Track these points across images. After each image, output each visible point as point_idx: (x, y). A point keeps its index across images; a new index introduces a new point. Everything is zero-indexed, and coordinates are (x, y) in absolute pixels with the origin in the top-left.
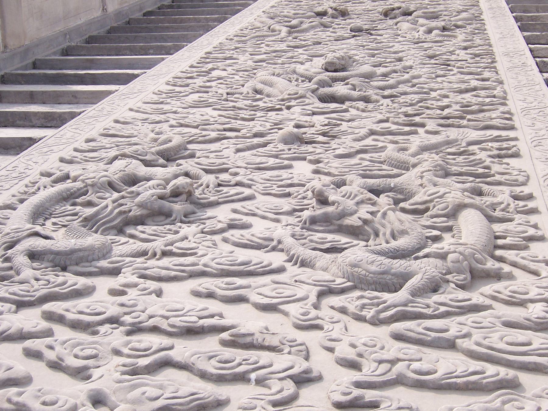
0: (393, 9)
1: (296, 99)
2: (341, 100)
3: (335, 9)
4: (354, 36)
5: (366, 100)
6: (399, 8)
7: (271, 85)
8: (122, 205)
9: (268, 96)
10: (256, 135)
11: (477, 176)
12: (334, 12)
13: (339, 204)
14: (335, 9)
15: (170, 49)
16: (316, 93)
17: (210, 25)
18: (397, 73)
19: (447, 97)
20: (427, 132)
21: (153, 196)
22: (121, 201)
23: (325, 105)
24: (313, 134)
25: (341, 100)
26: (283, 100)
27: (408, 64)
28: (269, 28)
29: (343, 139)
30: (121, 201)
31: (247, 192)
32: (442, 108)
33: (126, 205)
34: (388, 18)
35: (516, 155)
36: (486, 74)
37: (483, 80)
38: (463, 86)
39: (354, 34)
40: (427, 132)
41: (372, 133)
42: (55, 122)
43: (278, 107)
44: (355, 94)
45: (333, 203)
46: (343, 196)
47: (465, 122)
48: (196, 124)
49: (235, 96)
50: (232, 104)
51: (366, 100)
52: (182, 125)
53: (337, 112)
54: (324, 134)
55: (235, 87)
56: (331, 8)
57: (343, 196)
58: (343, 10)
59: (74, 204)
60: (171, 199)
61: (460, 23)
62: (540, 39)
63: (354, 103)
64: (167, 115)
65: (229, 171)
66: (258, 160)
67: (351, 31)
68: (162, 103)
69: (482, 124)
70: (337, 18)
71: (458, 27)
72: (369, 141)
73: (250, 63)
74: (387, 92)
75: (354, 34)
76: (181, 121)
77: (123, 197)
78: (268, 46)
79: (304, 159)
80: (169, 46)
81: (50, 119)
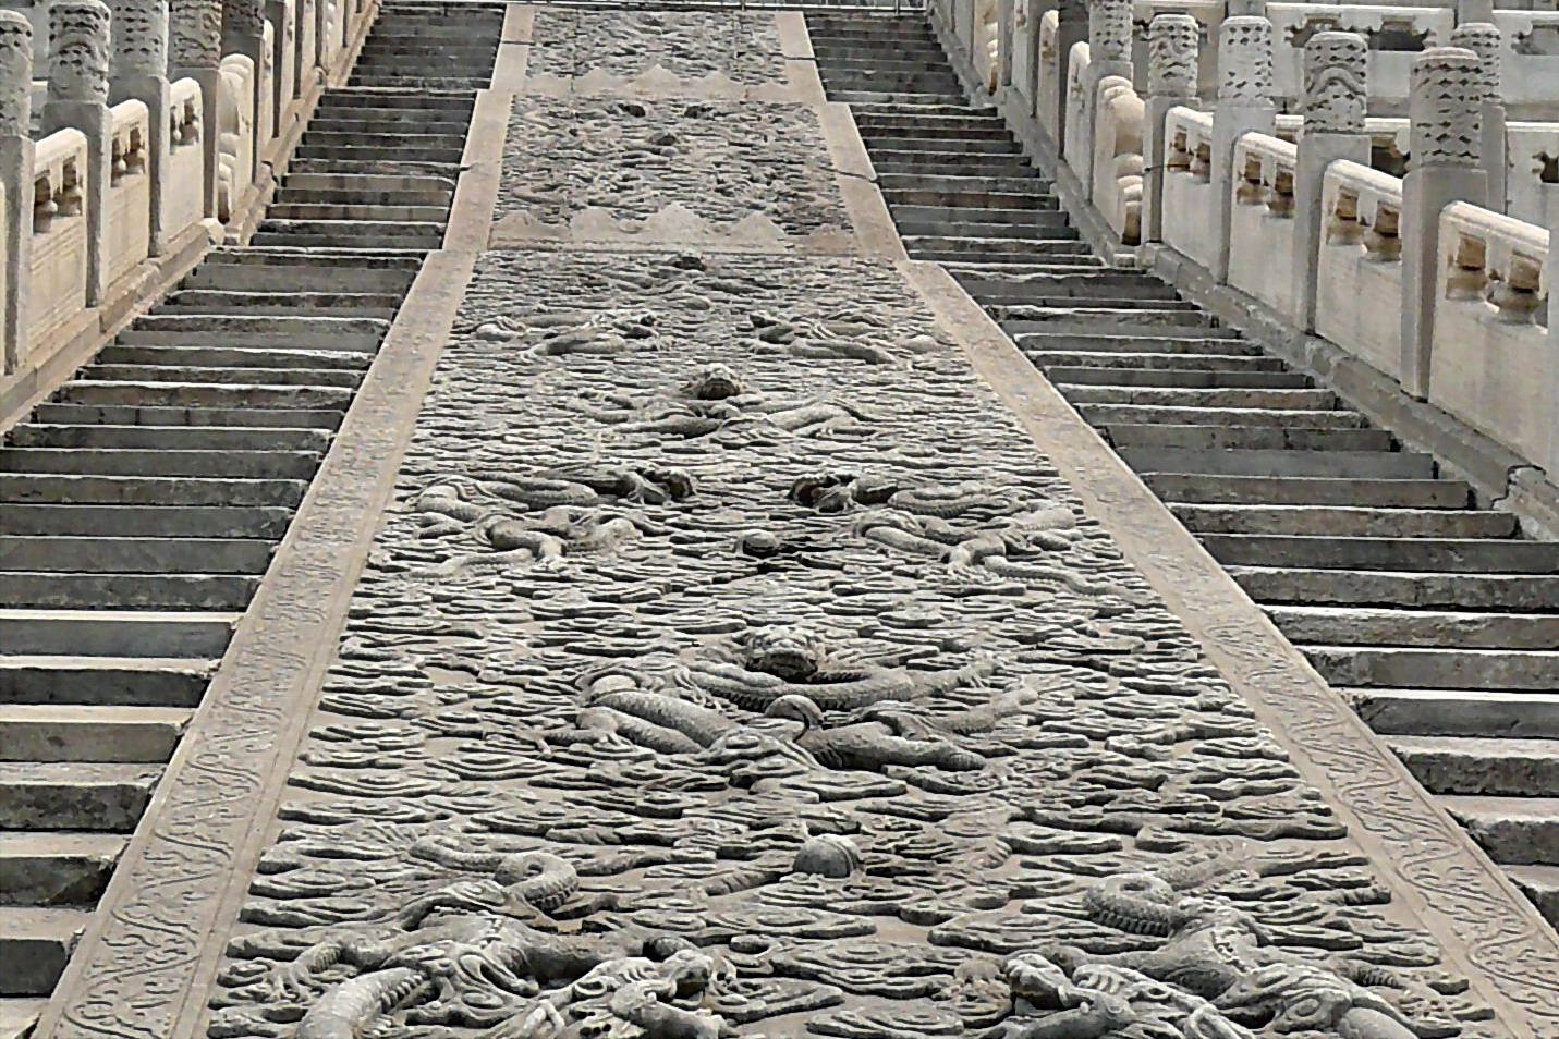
0: (830, 482)
1: (756, 758)
2: (875, 762)
3: (651, 477)
4: (763, 569)
5: (944, 762)
6: (846, 480)
7: (658, 718)
8: (582, 1015)
9: (665, 749)
10: (723, 854)
11: (1331, 945)
12: (648, 484)
13: (1090, 1003)
14: (651, 477)
15: (205, 594)
16: (802, 740)
17: (266, 513)
18: (967, 685)
19: (1140, 754)
20: (1142, 846)
21: (646, 993)
22: (579, 1006)
23: (842, 776)
24: (874, 850)
25: (875, 762)
26: (718, 761)
27: (984, 659)
28: (489, 533)
29: (958, 863)
30: (579, 1006)
31: (824, 991)
32: (1154, 784)
33: (592, 1014)
34: (816, 510)
35: (1382, 899)
36: (1208, 696)
37: (1205, 709)
38: (1170, 728)
39: (759, 561)
40: (1142, 846)
41: (1018, 848)
42: (70, 815)
43: (718, 779)
44: (918, 746)
45: (1075, 1003)
46: (1094, 987)
47: (1219, 820)
48: (534, 825)
49: (573, 748)
50: (581, 772)
51: (944, 762)
52: (494, 829)
53: (882, 794)
54: (899, 850)
55: (551, 722)
56: (639, 471)
57: (1094, 987)
58: (676, 481)
59: (412, 1021)
60: (677, 1001)
61: (1045, 535)
62: (1276, 588)
63: (913, 772)
64: (428, 797)
65: (734, 940)
66: (795, 914)
67: (746, 551)
68: (371, 764)
69: (1273, 825)
70: (659, 504)
71: (1047, 546)
72: (1014, 871)
73: (523, 648)
74: (984, 742)
75: (759, 561)
76: (486, 816)
77: (576, 997)
78: (527, 593)
79: (897, 913)
80: (203, 582)
81: (53, 806)
